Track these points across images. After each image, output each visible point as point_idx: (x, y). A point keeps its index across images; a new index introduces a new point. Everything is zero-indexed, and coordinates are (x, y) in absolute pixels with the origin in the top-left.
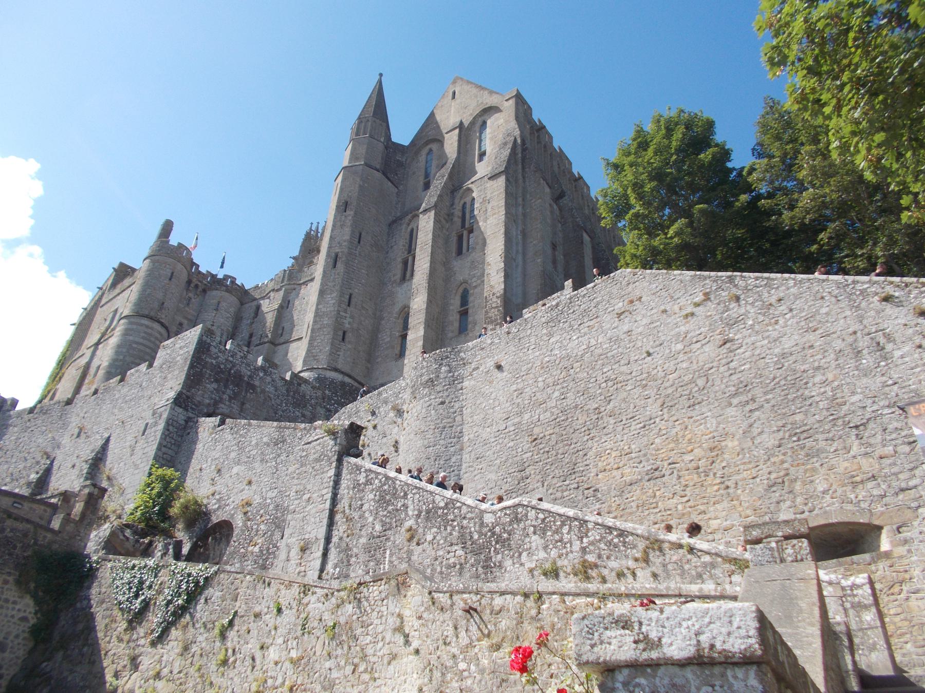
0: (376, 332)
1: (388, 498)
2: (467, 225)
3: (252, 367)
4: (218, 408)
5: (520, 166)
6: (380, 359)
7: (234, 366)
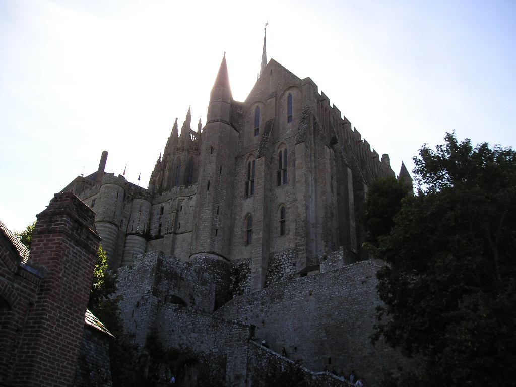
0: (232, 228)
1: (273, 362)
2: (283, 168)
5: (313, 135)
6: (236, 244)
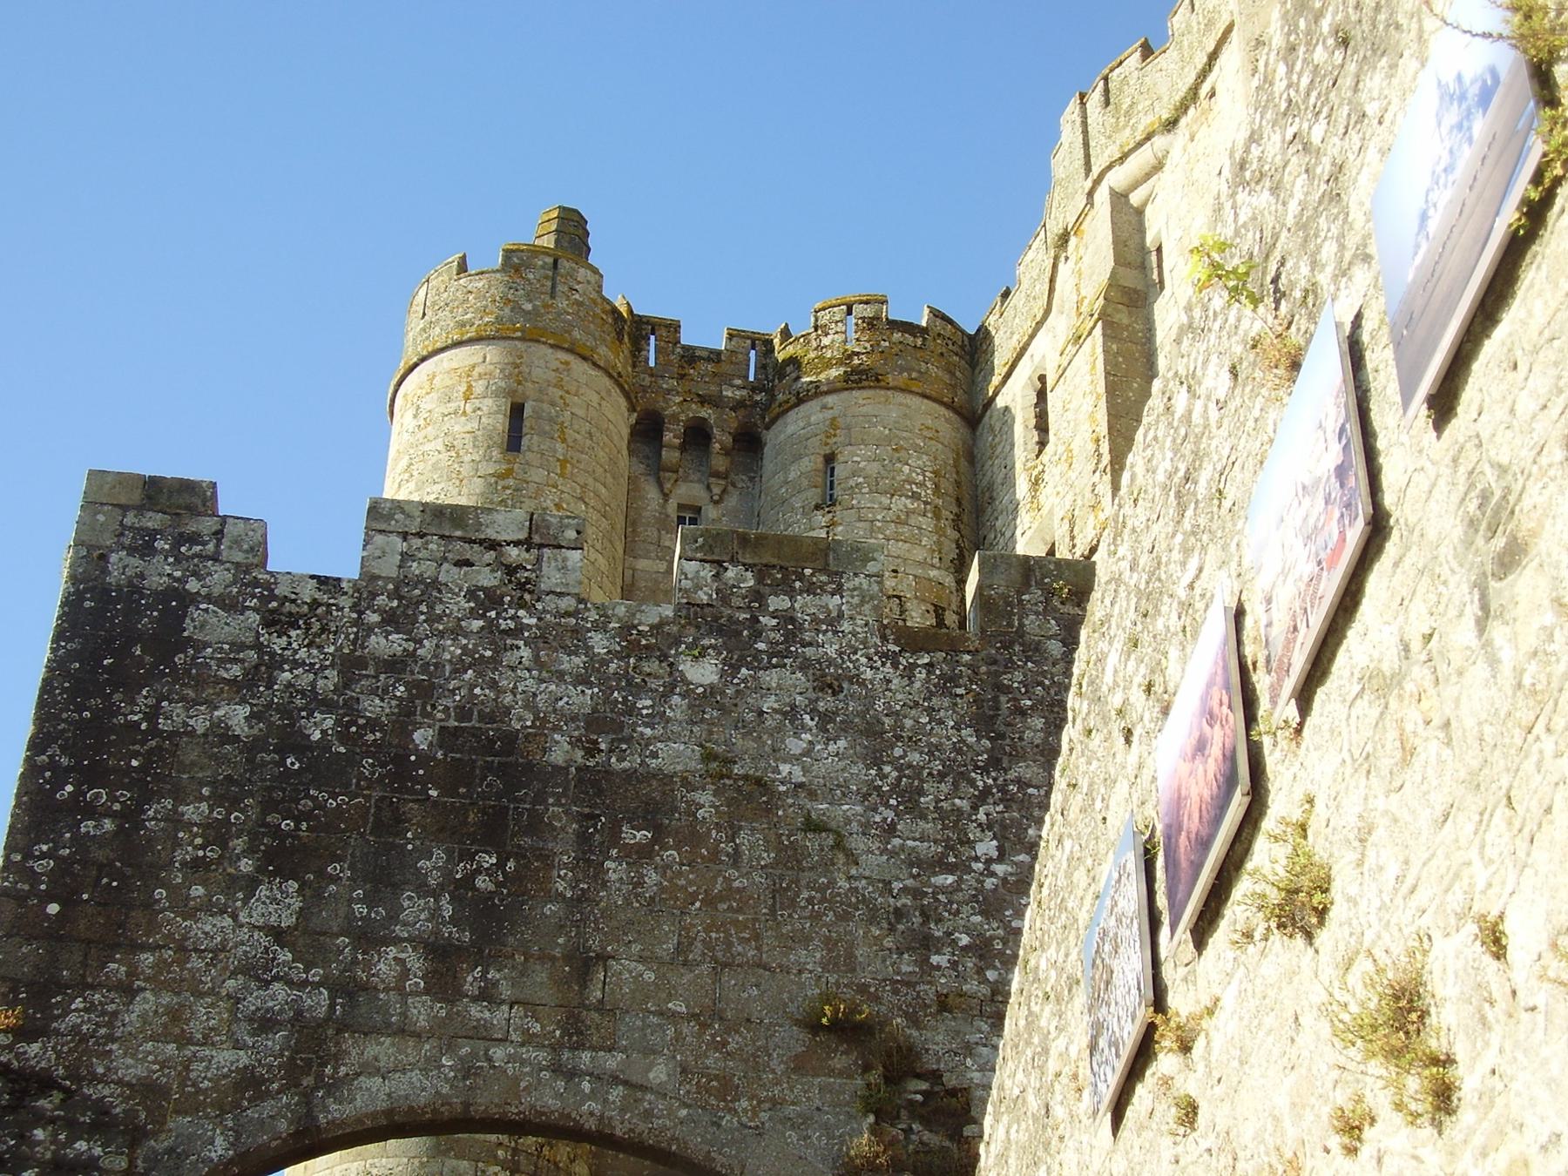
3: (600, 644)
4: (334, 1087)
7: (425, 692)
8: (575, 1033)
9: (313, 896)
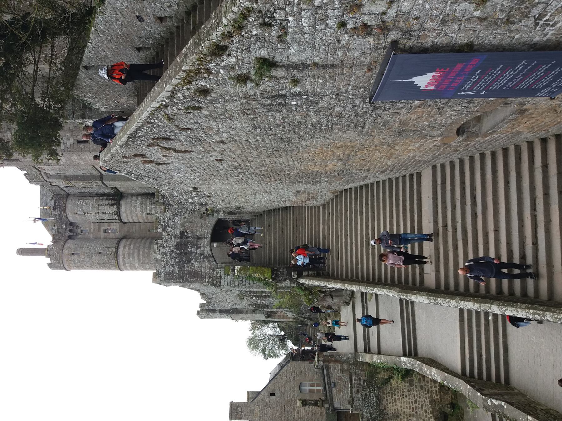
3: (167, 238)
4: (209, 255)
7: (173, 252)
8: (204, 238)
9: (193, 259)
